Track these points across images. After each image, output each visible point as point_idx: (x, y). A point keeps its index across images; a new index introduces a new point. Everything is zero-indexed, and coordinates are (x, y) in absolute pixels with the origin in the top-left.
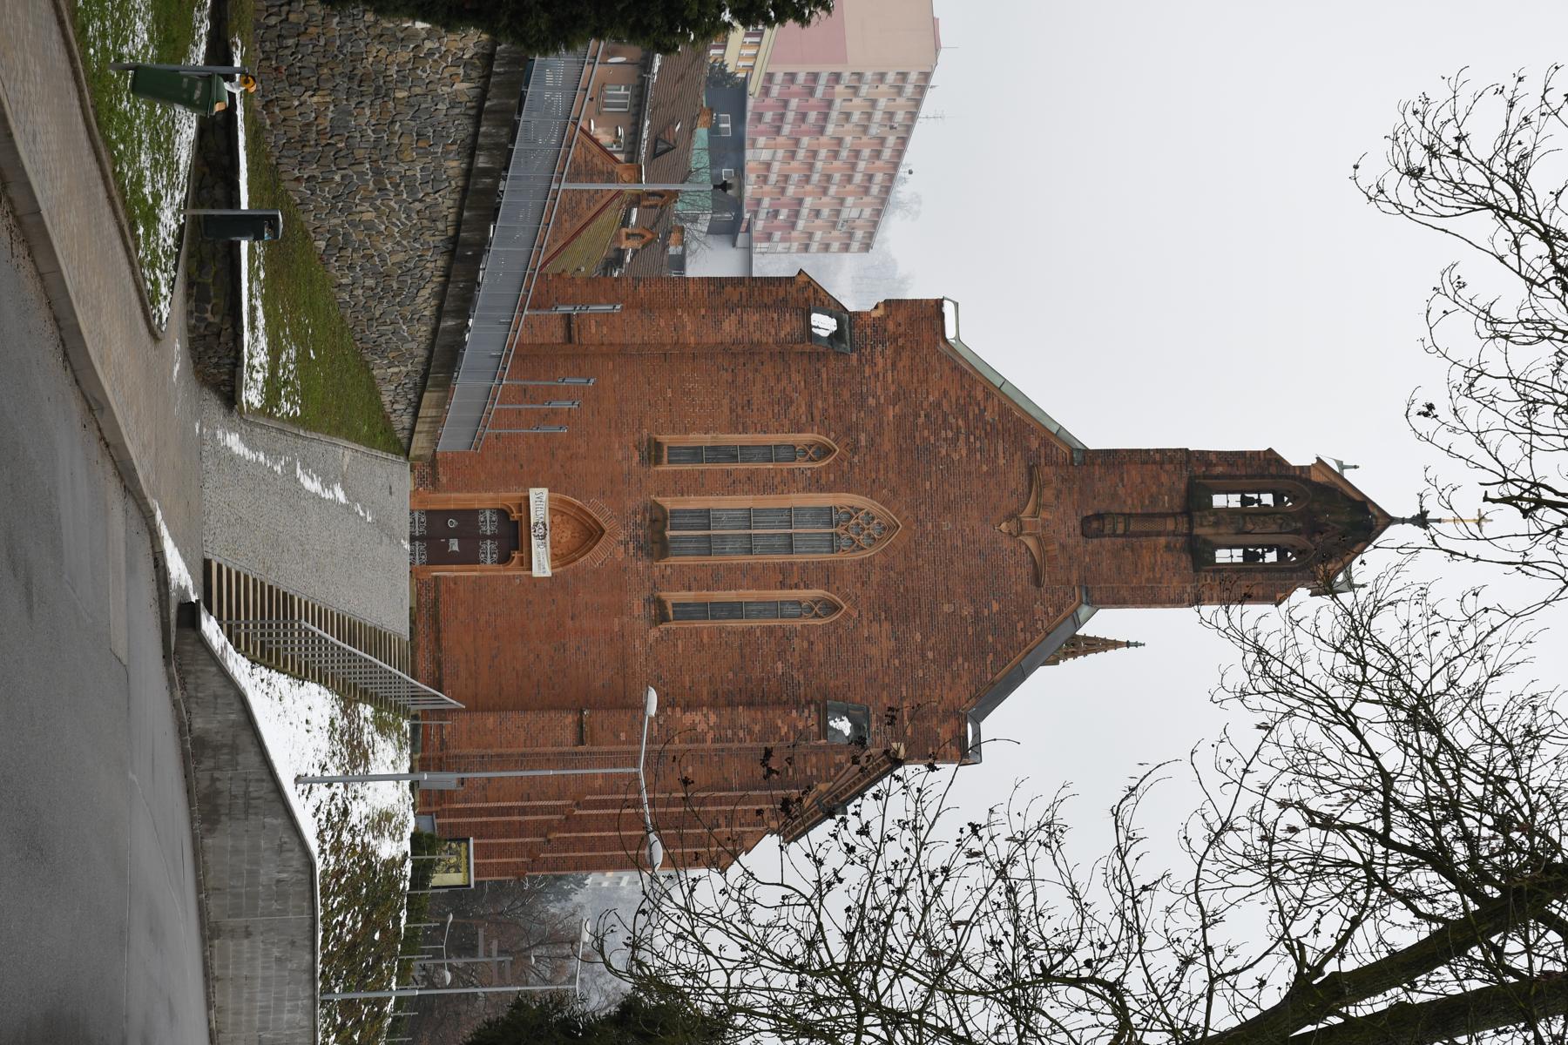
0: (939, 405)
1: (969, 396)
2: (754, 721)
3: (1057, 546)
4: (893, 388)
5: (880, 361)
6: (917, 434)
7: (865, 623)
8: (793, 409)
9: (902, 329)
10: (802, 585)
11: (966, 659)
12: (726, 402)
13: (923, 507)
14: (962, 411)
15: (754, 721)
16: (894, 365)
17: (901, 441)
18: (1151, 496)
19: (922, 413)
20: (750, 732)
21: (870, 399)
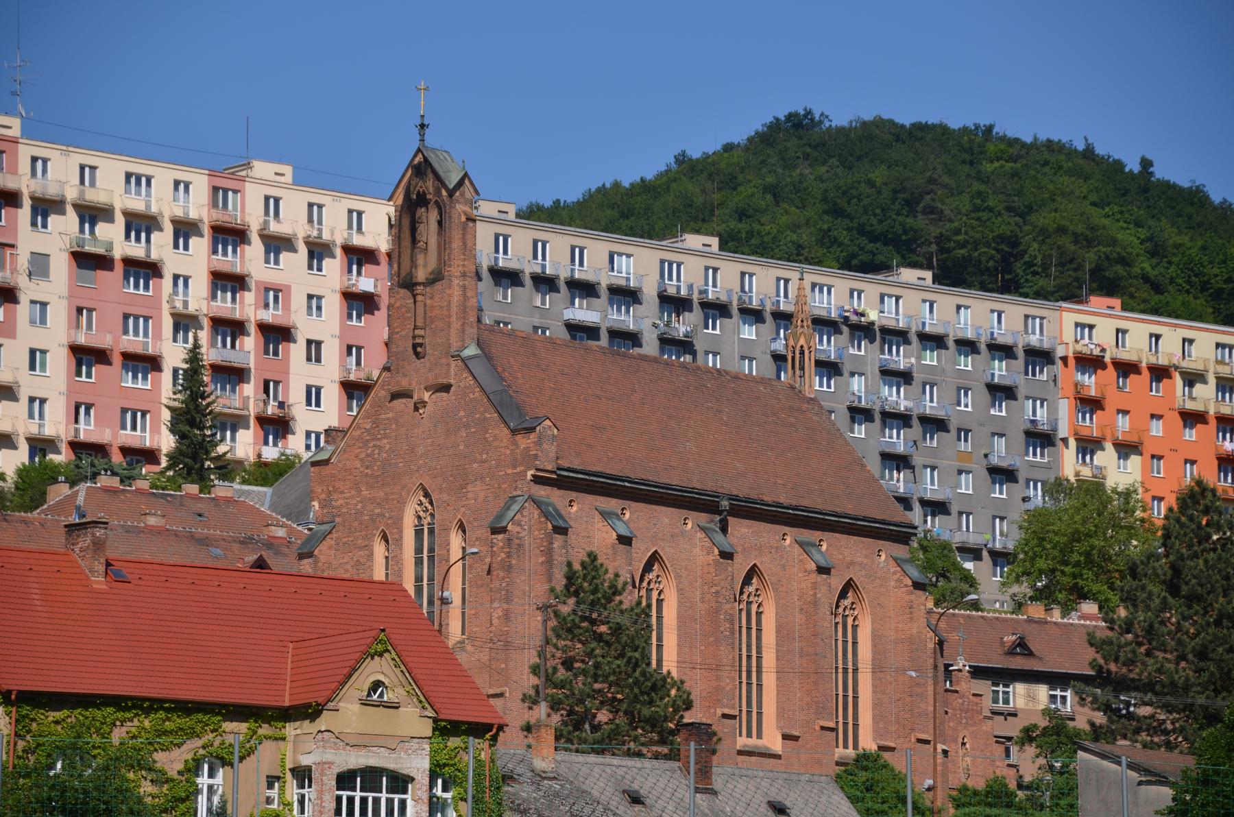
0: (362, 460)
4: (353, 492)
8: (361, 560)
15: (498, 576)
16: (342, 493)
20: (503, 578)
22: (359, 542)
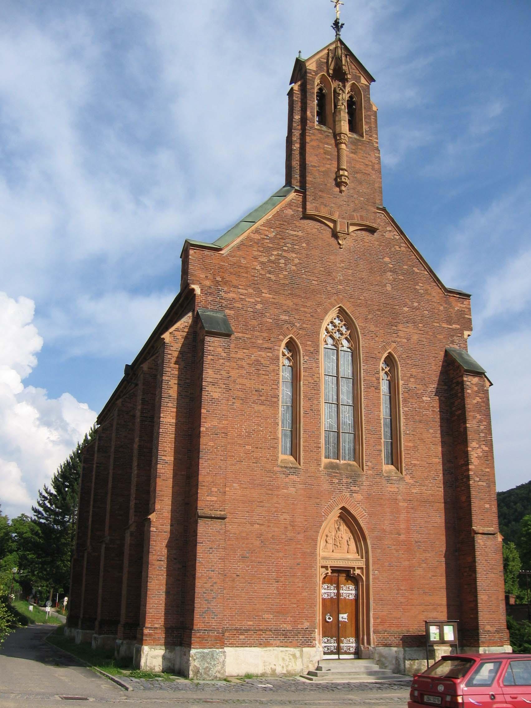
0: (262, 263)
2: (475, 417)
3: (355, 214)
4: (251, 291)
5: (231, 295)
6: (282, 282)
7: (399, 340)
8: (262, 360)
9: (210, 276)
10: (377, 375)
11: (417, 284)
12: (257, 408)
13: (329, 289)
15: (475, 417)
16: (235, 287)
18: (324, 153)
19: (268, 275)
21: (257, 307)
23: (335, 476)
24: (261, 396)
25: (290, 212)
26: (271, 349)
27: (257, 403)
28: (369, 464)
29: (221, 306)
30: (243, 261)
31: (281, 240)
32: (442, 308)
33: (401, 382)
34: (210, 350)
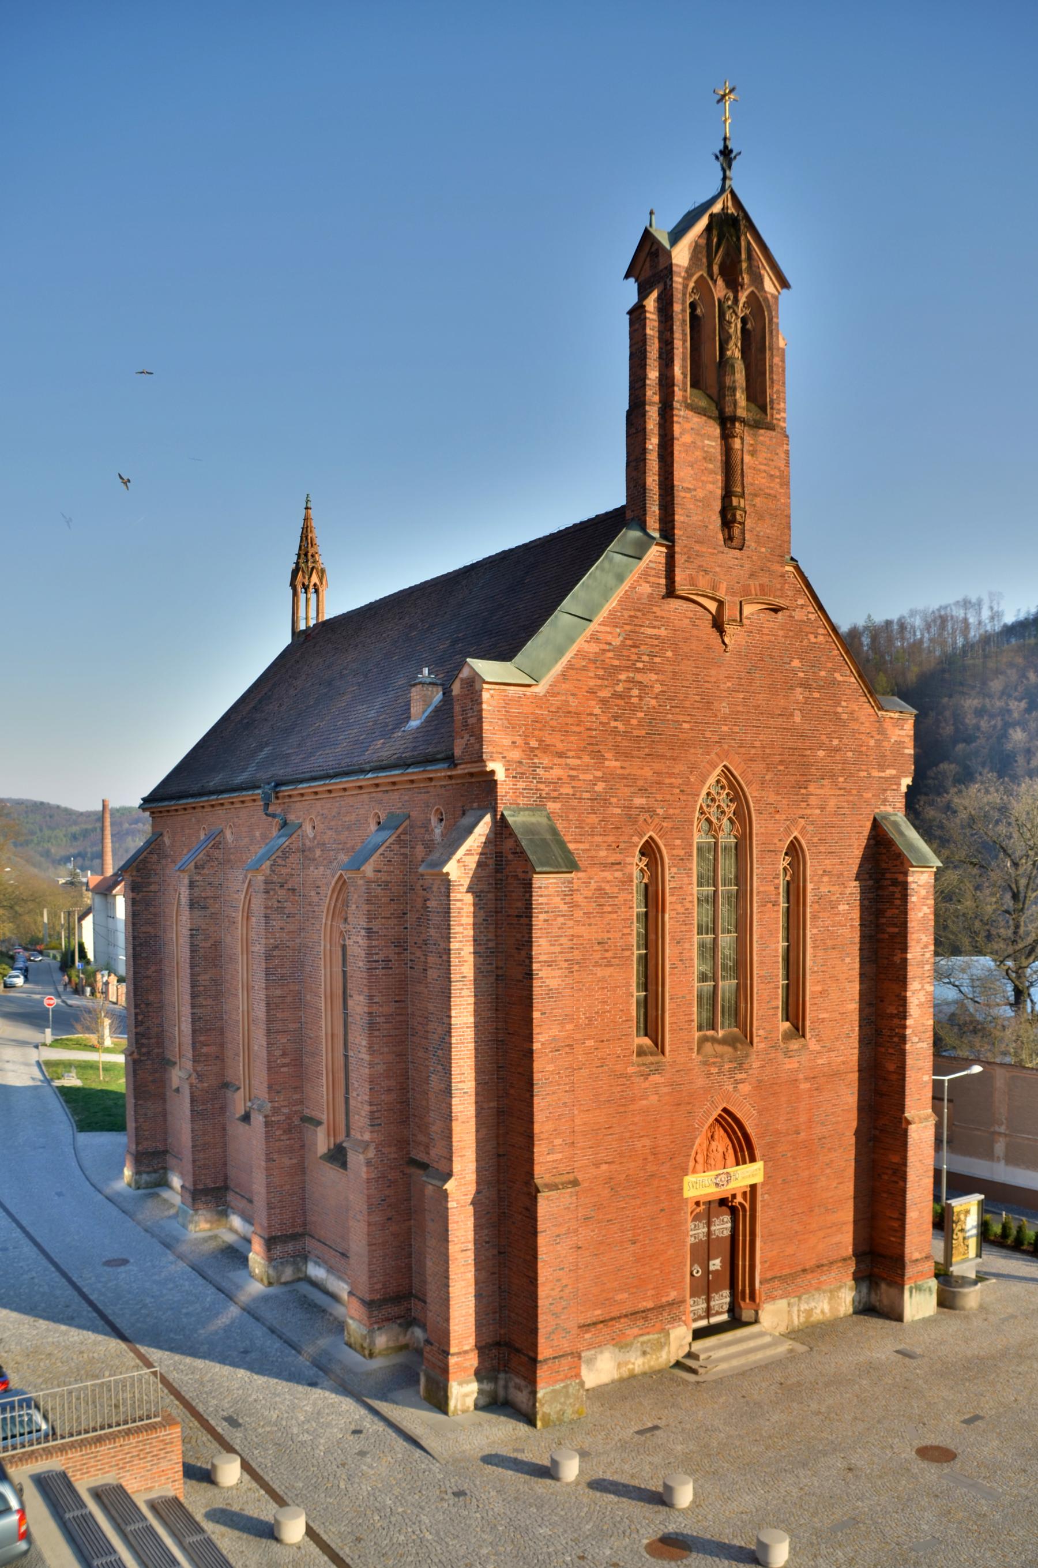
0: (604, 701)
1: (595, 661)
3: (751, 582)
4: (587, 759)
5: (556, 772)
6: (636, 733)
7: (809, 812)
9: (519, 741)
12: (600, 972)
13: (708, 734)
14: (611, 672)
15: (918, 941)
16: (561, 755)
17: (642, 754)
22: (603, 853)
23: (714, 1063)
24: (607, 951)
25: (645, 589)
26: (620, 863)
27: (601, 965)
28: (761, 1032)
29: (540, 797)
30: (573, 702)
31: (633, 650)
32: (872, 742)
33: (810, 886)
34: (541, 904)
